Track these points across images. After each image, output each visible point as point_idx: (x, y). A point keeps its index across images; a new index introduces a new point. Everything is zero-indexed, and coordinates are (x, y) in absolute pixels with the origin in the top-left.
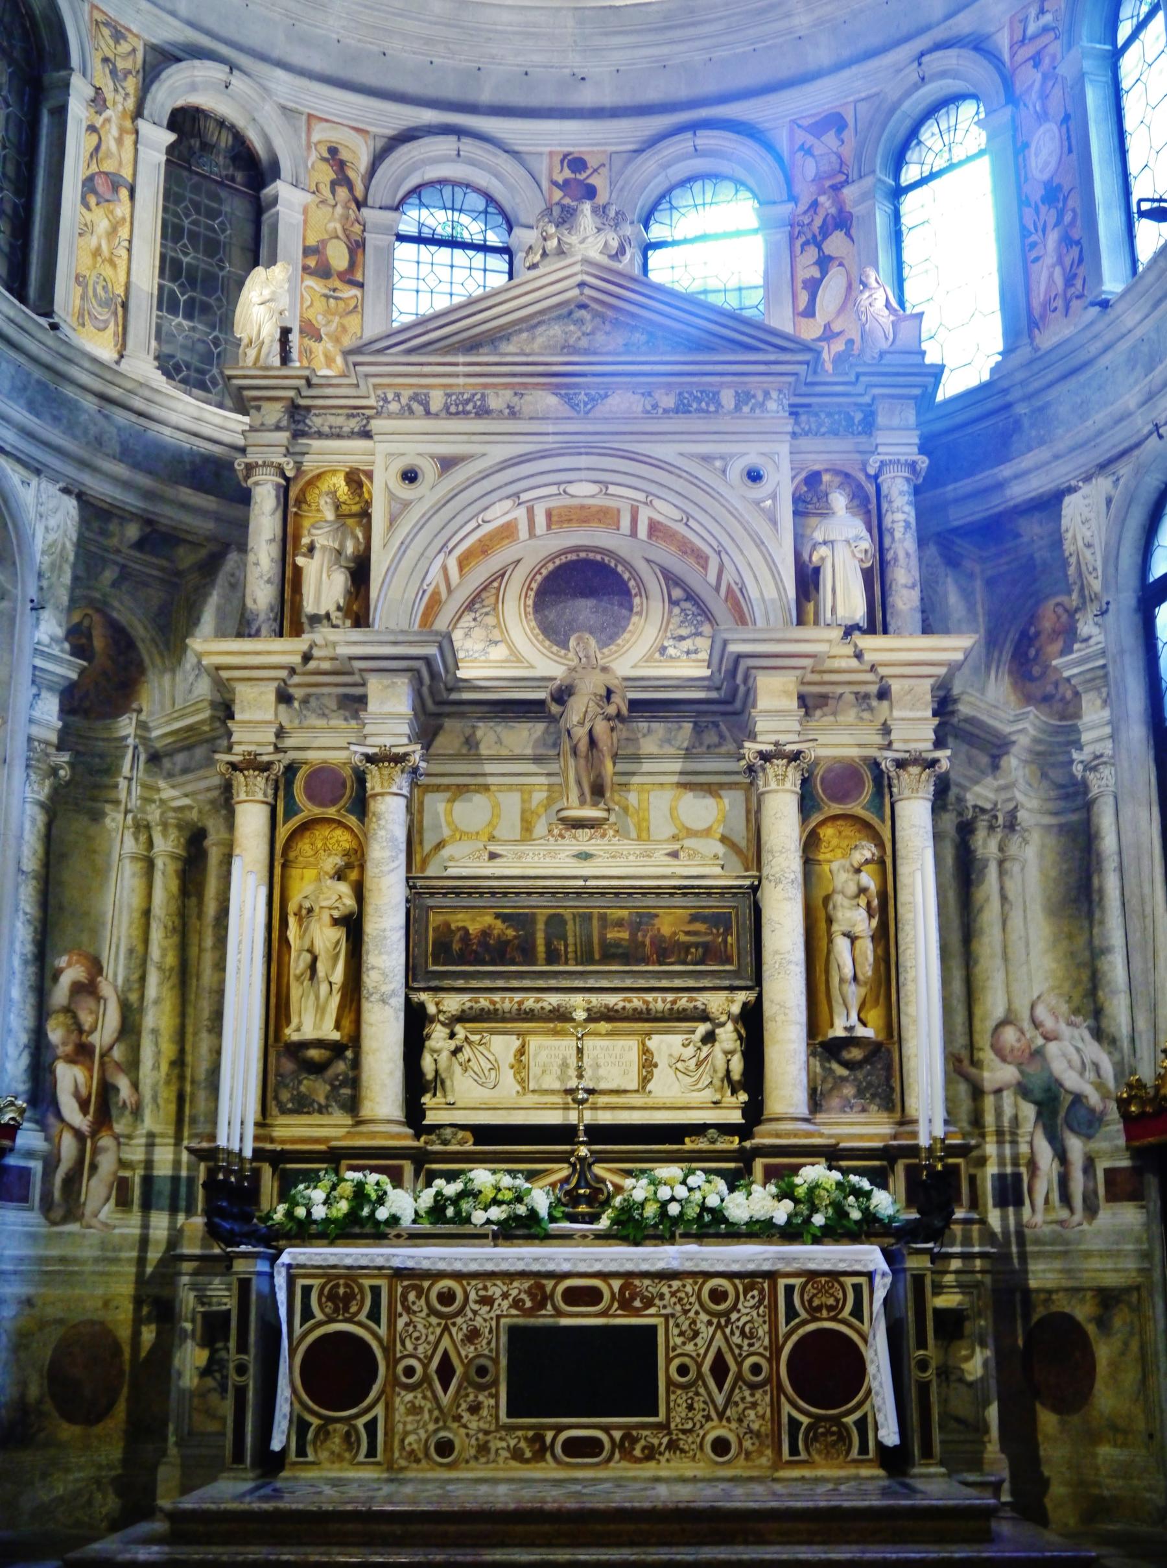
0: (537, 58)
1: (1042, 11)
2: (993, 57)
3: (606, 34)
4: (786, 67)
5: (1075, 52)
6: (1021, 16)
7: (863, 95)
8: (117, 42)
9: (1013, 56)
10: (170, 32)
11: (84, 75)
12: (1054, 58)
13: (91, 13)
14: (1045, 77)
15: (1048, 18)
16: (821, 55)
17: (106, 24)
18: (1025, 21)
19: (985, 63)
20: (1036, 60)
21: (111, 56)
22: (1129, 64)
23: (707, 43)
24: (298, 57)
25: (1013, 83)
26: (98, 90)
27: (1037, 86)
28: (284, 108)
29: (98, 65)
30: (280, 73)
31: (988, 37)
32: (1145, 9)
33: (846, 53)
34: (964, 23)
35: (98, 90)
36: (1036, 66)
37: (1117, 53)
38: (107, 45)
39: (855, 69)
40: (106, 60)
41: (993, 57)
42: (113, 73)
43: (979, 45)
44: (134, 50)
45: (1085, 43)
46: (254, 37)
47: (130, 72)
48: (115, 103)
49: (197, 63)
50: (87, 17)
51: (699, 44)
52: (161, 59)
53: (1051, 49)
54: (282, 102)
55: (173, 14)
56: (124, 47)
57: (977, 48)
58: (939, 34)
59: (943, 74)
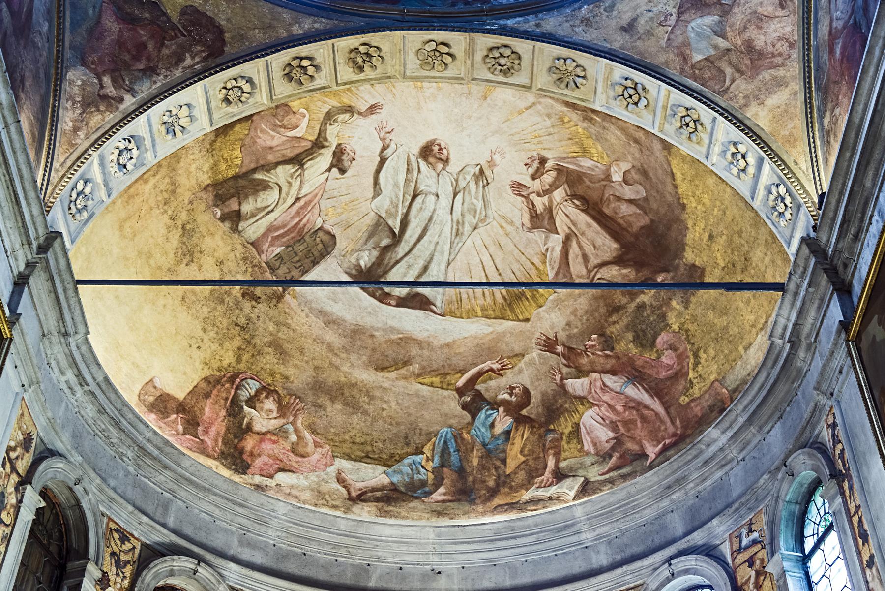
0: (409, 558)
1: (751, 531)
2: (720, 560)
3: (455, 543)
4: (578, 567)
5: (777, 557)
6: (736, 534)
7: (632, 585)
8: (123, 543)
9: (733, 560)
10: (161, 536)
11: (97, 564)
12: (762, 560)
13: (108, 524)
14: (758, 574)
15: (755, 535)
16: (602, 559)
17: (117, 531)
18: (740, 537)
19: (715, 564)
20: (751, 562)
21: (117, 551)
22: (815, 565)
23: (523, 550)
24: (246, 554)
25: (736, 578)
26: (105, 573)
27: (752, 580)
28: (232, 588)
29: (107, 557)
30: (232, 565)
31: (716, 547)
32: (822, 530)
33: (618, 557)
34: (698, 538)
35: (105, 573)
36: (751, 566)
37: (805, 559)
38: (115, 544)
39: (625, 568)
40: (113, 554)
41: (720, 560)
42: (118, 563)
43: (710, 552)
44: (134, 548)
45: (783, 551)
46: (218, 541)
47: (129, 562)
48: (115, 583)
49: (176, 557)
50: (104, 526)
51: (518, 551)
52: (151, 553)
53: (760, 555)
54: (232, 584)
55: (164, 525)
56: (128, 546)
57: (708, 555)
58: (681, 545)
59: (687, 572)
